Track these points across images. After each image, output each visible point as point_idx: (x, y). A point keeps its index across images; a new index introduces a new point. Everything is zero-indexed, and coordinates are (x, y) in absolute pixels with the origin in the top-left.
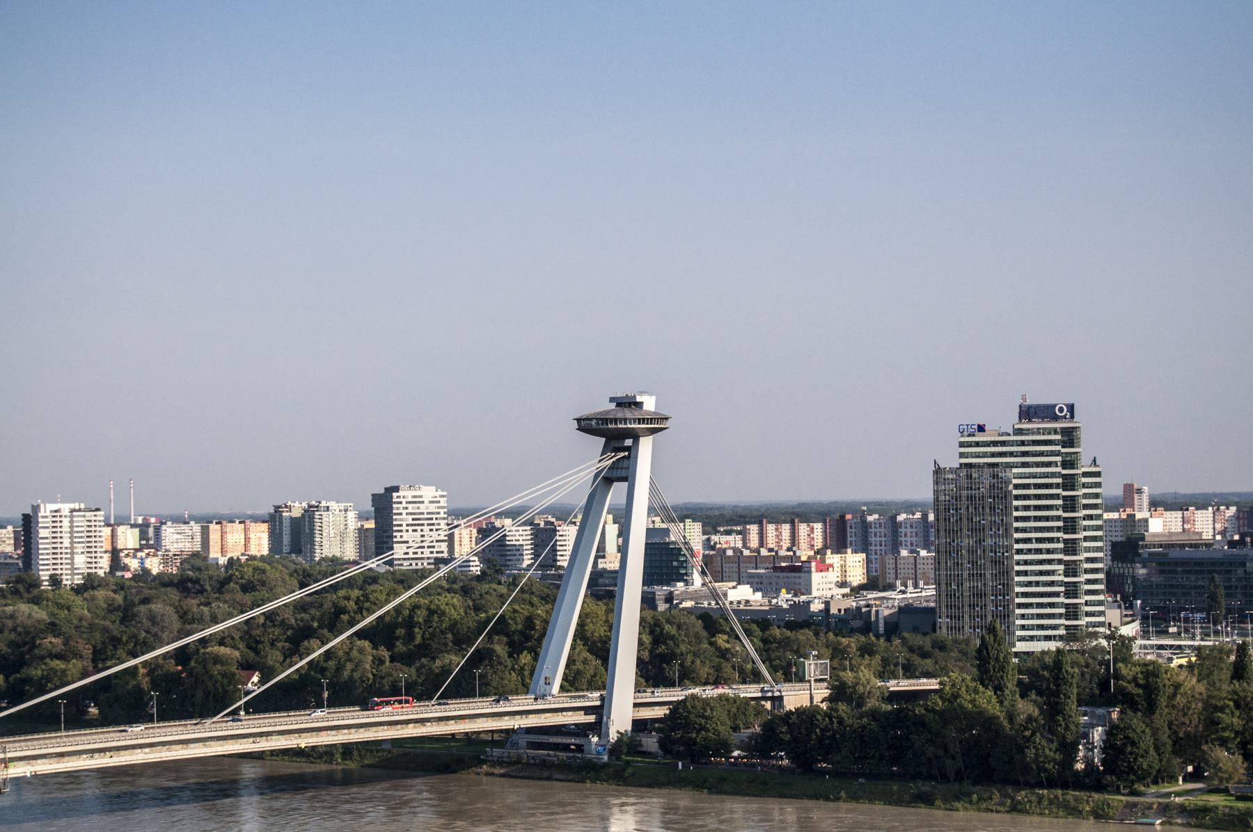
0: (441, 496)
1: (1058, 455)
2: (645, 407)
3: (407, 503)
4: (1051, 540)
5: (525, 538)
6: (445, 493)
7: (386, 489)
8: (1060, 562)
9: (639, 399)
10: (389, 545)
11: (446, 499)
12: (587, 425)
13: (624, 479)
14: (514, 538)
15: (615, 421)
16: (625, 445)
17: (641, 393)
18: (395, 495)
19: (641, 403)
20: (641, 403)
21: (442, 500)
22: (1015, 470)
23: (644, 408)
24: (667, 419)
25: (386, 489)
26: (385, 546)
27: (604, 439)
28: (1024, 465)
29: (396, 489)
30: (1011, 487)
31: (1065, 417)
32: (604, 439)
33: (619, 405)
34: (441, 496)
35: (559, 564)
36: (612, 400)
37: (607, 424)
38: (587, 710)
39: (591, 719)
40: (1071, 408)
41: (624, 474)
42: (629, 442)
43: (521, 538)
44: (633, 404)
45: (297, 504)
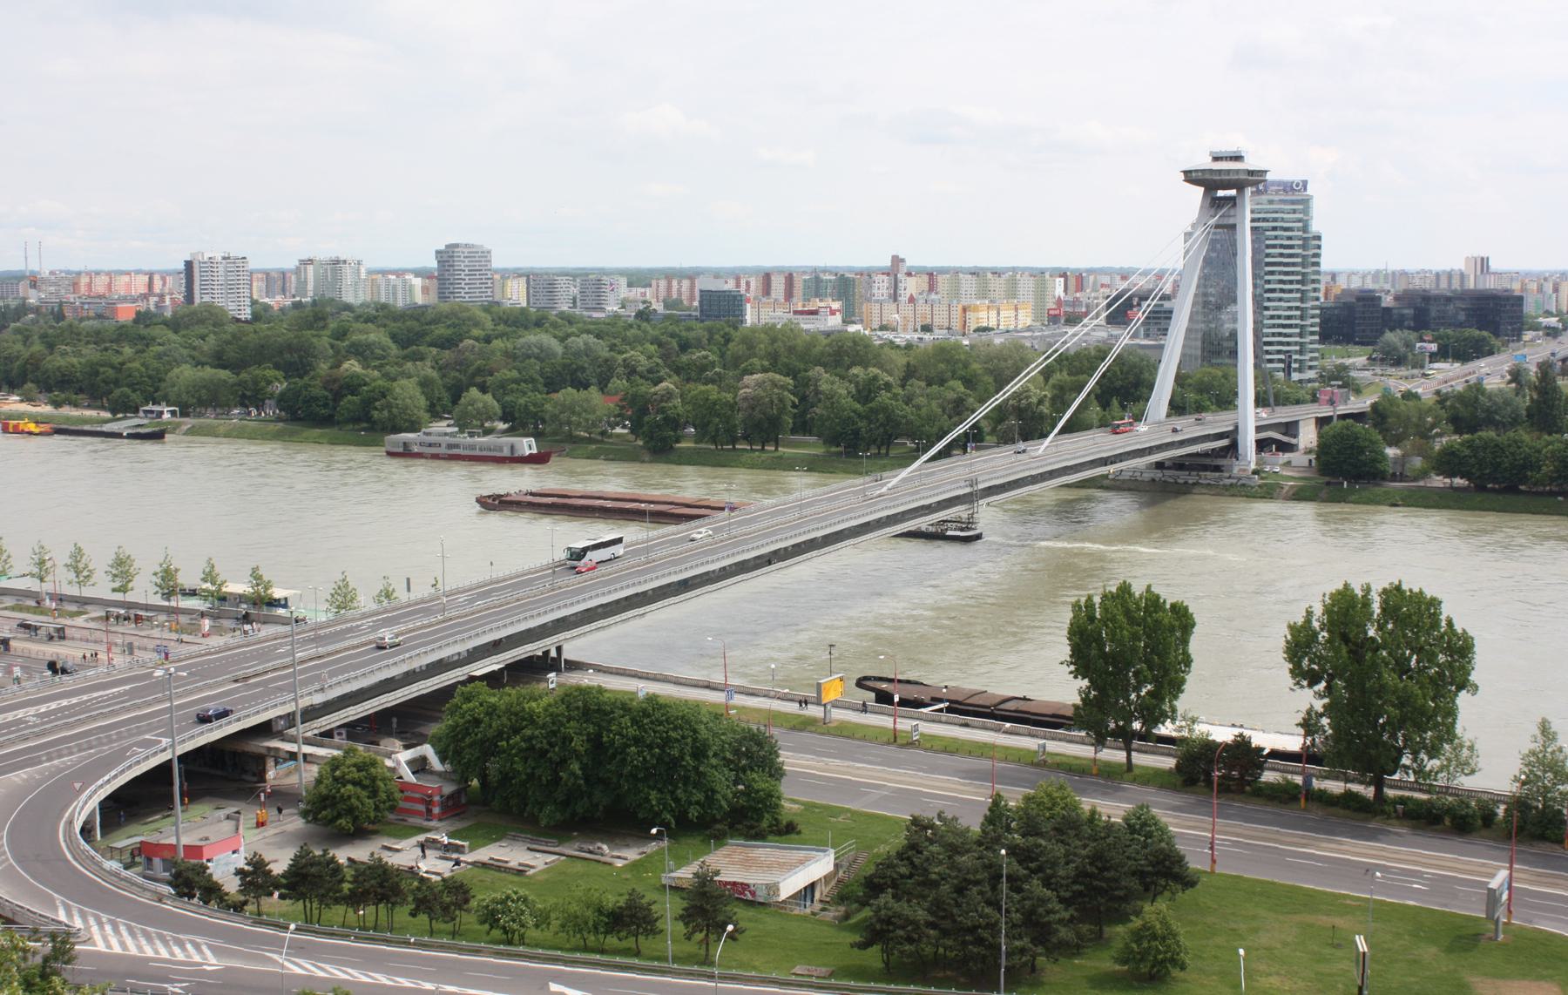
4: (1291, 291)
7: (447, 246)
8: (1297, 308)
12: (1191, 177)
15: (1211, 171)
22: (1268, 233)
24: (1266, 171)
27: (1203, 189)
28: (1274, 229)
30: (1264, 247)
31: (1299, 191)
32: (1203, 189)
40: (1305, 183)
41: (1231, 221)
42: (1233, 192)
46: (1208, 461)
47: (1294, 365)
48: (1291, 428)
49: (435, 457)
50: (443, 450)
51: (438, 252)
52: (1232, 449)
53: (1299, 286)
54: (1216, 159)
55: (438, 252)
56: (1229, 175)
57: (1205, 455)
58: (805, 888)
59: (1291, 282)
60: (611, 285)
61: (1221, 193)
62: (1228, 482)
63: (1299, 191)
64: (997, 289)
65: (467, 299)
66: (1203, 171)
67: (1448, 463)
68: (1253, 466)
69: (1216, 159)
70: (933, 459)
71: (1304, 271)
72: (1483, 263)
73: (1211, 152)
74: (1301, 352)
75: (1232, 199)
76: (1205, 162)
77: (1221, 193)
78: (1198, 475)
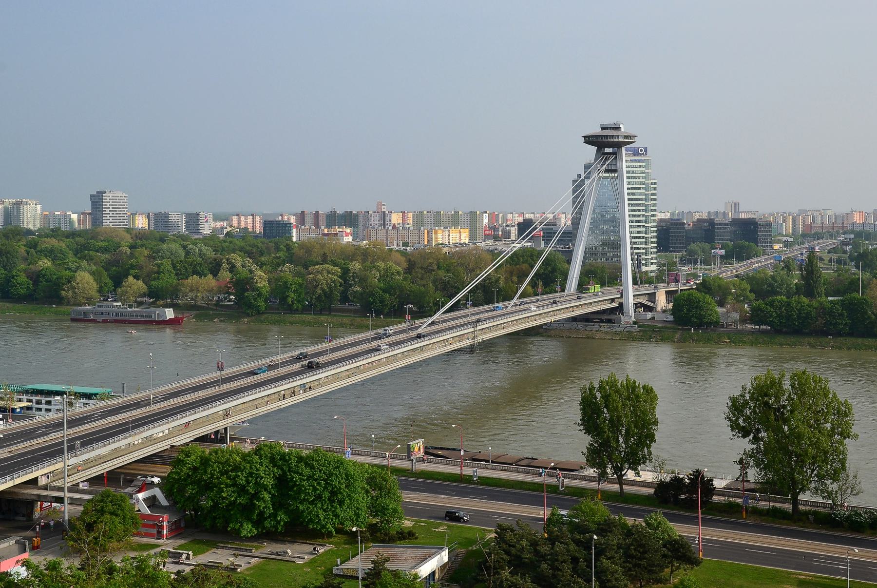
1: (644, 173)
4: (639, 216)
12: (589, 140)
13: (615, 171)
18: (104, 195)
21: (125, 198)
27: (596, 148)
29: (105, 192)
31: (643, 154)
32: (596, 148)
33: (603, 129)
37: (613, 138)
38: (613, 300)
39: (615, 305)
40: (646, 149)
43: (175, 218)
45: (7, 200)
47: (643, 262)
48: (652, 297)
49: (105, 321)
50: (111, 317)
51: (92, 196)
52: (620, 308)
53: (644, 213)
54: (603, 129)
55: (92, 196)
56: (613, 138)
57: (604, 311)
58: (429, 575)
59: (639, 210)
60: (206, 217)
61: (607, 150)
62: (618, 329)
63: (643, 154)
64: (447, 221)
66: (596, 136)
67: (756, 317)
68: (633, 319)
70: (445, 312)
71: (646, 203)
72: (737, 205)
74: (646, 254)
76: (597, 131)
77: (607, 150)
78: (599, 325)
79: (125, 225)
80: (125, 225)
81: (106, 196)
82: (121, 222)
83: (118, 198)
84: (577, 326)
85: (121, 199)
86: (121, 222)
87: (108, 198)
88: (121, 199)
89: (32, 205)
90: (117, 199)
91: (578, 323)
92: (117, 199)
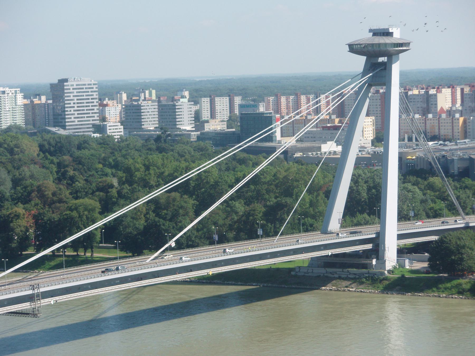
0: (94, 84)
2: (395, 35)
3: (73, 89)
5: (146, 111)
6: (96, 83)
7: (59, 80)
9: (391, 31)
10: (63, 117)
11: (97, 86)
14: (146, 111)
16: (379, 61)
17: (392, 26)
18: (65, 84)
19: (392, 33)
20: (392, 33)
21: (95, 86)
23: (394, 36)
25: (59, 80)
26: (60, 117)
27: (365, 58)
29: (66, 80)
32: (365, 58)
34: (94, 84)
35: (178, 127)
36: (370, 31)
44: (387, 34)
46: (357, 261)
57: (355, 255)
61: (381, 59)
65: (76, 123)
69: (376, 33)
73: (370, 31)
75: (383, 64)
77: (381, 59)
79: (95, 120)
80: (95, 120)
81: (68, 85)
82: (90, 117)
83: (84, 87)
84: (327, 272)
85: (89, 88)
86: (90, 117)
87: (71, 88)
88: (89, 88)
89: (10, 94)
90: (83, 88)
91: (326, 269)
92: (83, 88)
